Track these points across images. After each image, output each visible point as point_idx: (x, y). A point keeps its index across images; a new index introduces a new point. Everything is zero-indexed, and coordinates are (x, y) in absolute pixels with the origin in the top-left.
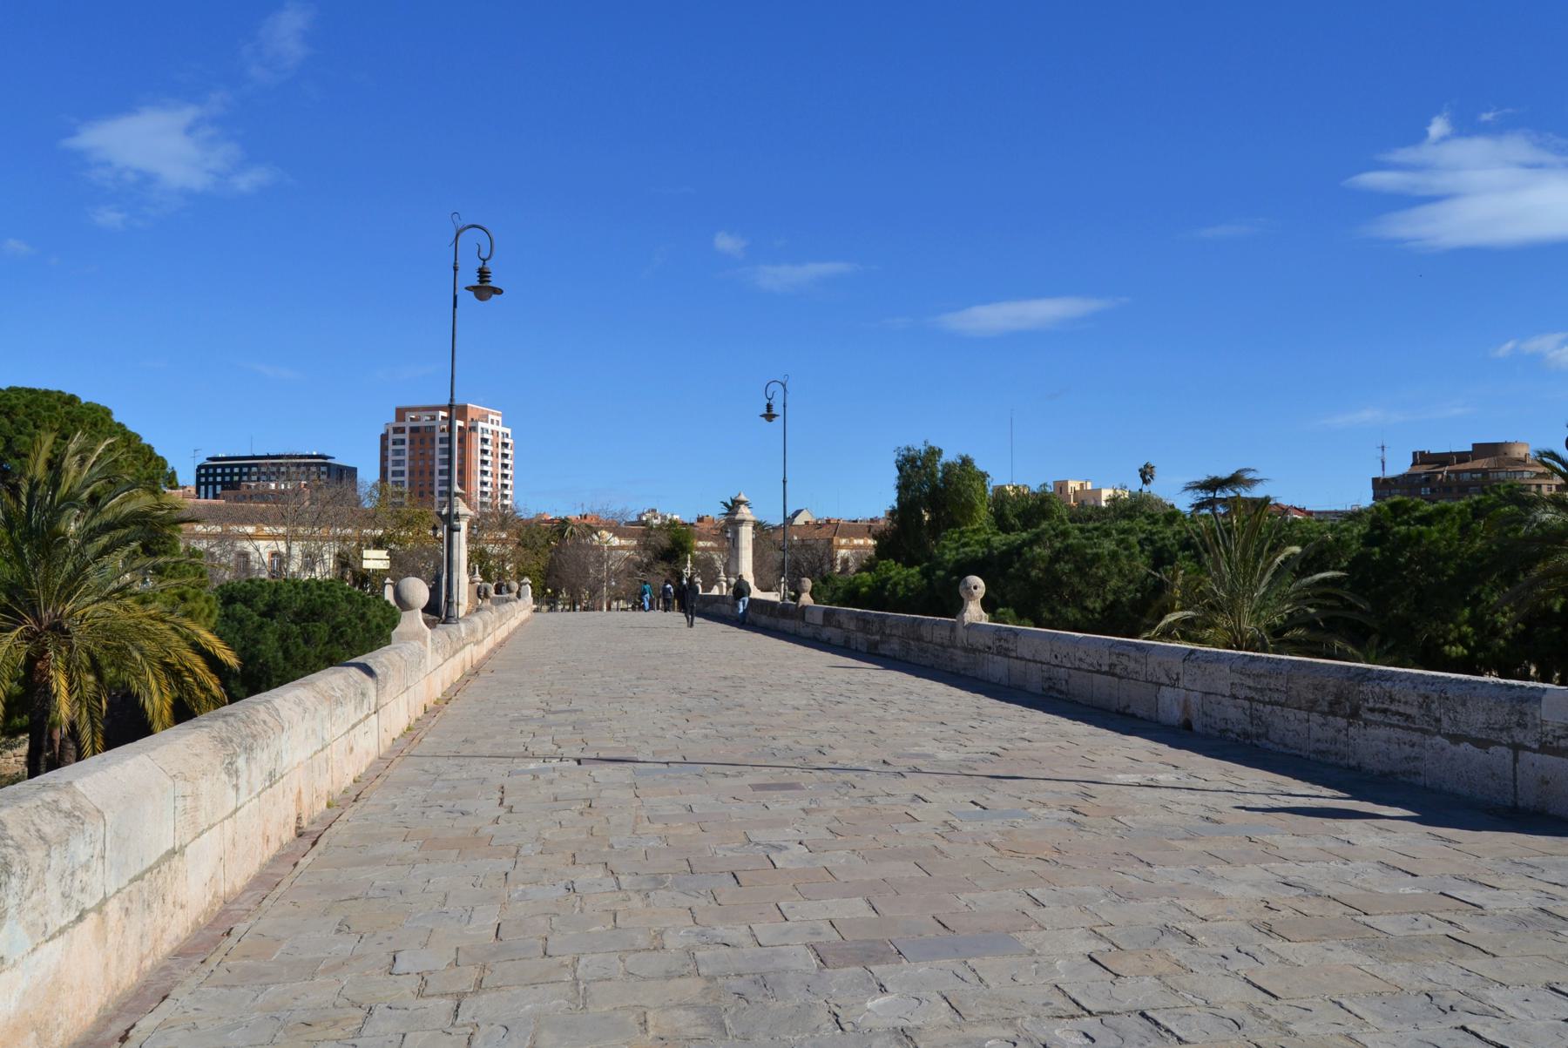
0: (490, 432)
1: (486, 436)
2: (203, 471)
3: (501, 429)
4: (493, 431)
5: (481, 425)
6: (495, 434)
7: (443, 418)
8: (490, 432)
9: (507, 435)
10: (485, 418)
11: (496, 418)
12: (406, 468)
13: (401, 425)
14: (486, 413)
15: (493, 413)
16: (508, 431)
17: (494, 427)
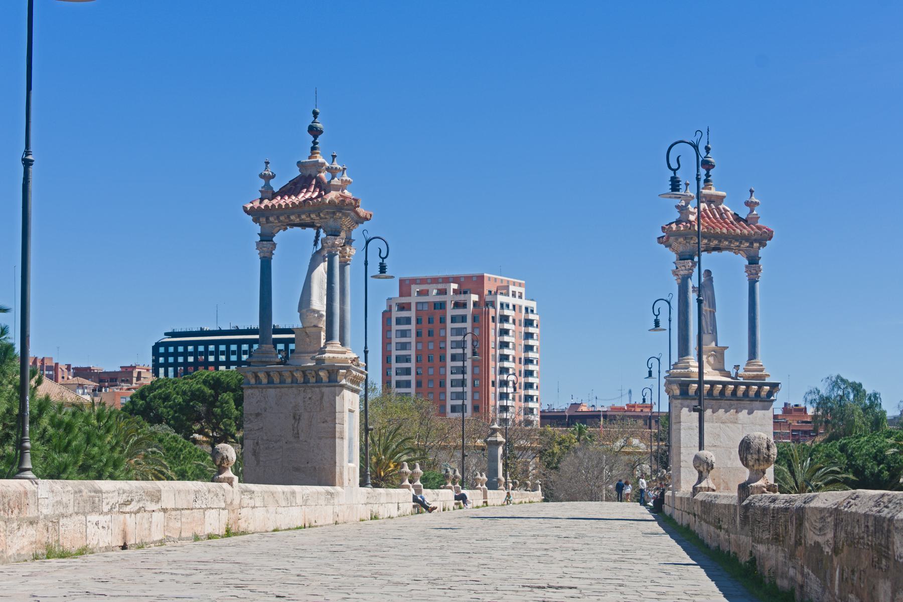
0: (511, 307)
1: (506, 312)
2: (162, 350)
3: (524, 303)
4: (514, 306)
5: (500, 299)
6: (517, 308)
7: (454, 290)
8: (511, 307)
9: (532, 311)
10: (504, 289)
11: (518, 289)
12: (412, 352)
13: (405, 300)
14: (505, 284)
15: (514, 284)
16: (533, 304)
17: (516, 301)
